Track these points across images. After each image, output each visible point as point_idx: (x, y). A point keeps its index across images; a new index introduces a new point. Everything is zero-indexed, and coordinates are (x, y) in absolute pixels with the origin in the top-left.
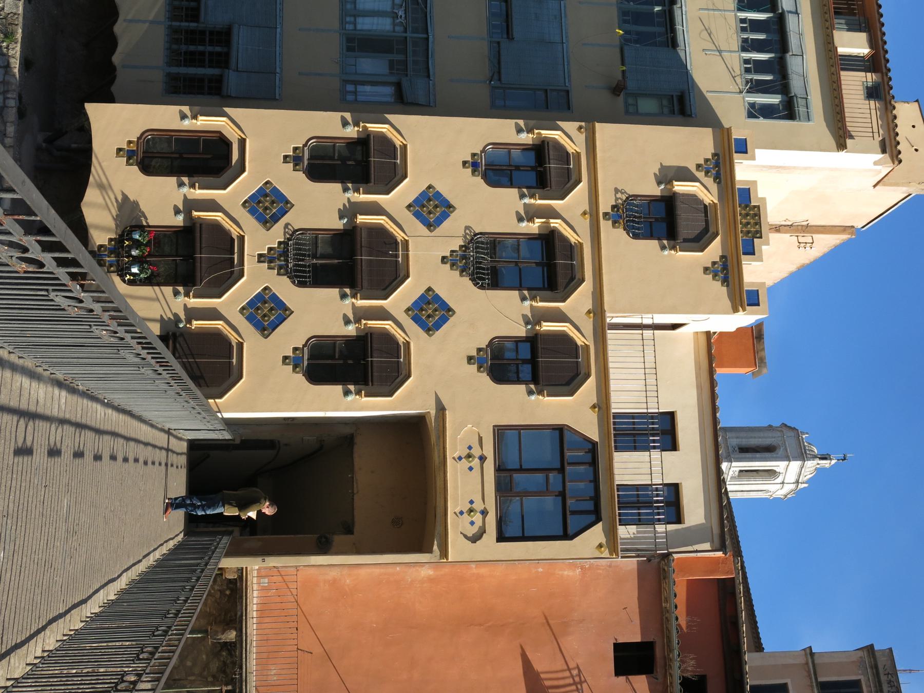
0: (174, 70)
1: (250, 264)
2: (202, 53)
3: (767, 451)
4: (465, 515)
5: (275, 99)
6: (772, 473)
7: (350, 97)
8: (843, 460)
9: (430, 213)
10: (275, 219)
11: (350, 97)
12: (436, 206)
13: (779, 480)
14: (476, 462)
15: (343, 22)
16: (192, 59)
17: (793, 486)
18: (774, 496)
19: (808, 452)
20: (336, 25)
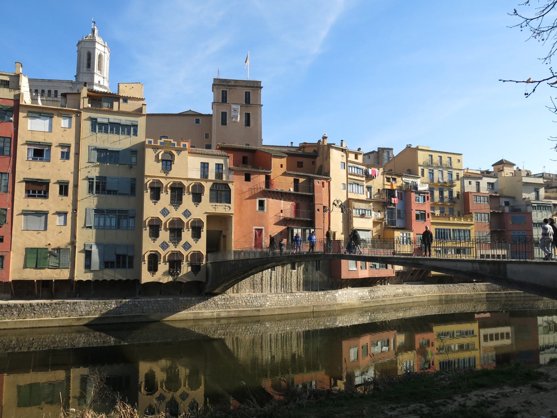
0: (127, 266)
1: (177, 249)
2: (123, 261)
3: (90, 57)
6: (100, 56)
8: (95, 23)
10: (167, 244)
11: (133, 228)
13: (103, 54)
14: (216, 207)
15: (113, 229)
16: (124, 263)
17: (106, 48)
18: (109, 57)
19: (91, 39)
20: (115, 231)
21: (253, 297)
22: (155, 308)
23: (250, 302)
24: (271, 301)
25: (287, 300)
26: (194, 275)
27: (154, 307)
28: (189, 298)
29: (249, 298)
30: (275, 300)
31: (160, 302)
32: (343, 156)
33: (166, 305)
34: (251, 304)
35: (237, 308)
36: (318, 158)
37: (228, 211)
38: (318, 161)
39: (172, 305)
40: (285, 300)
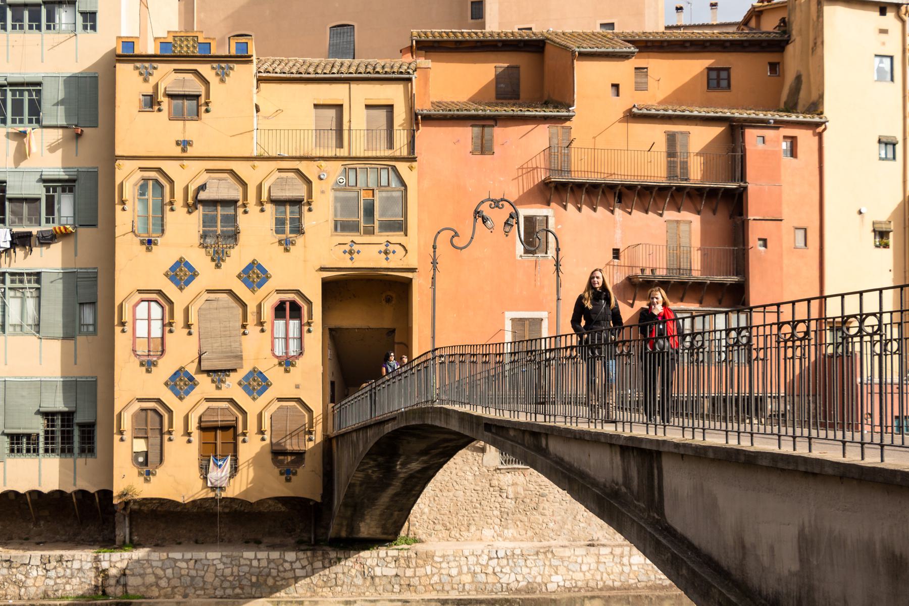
0: (76, 450)
1: (224, 393)
2: (63, 432)
4: (389, 256)
5: (96, 381)
9: (185, 275)
10: (191, 379)
11: (91, 329)
12: (181, 270)
14: (356, 248)
16: (67, 437)
21: (501, 554)
22: (163, 583)
23: (490, 570)
24: (568, 570)
25: (635, 568)
26: (284, 477)
27: (161, 578)
28: (275, 555)
29: (486, 558)
30: (585, 568)
31: (179, 564)
32: (884, 31)
33: (202, 573)
34: (491, 579)
35: (443, 590)
36: (790, 49)
37: (396, 261)
38: (792, 58)
39: (219, 573)
40: (627, 569)
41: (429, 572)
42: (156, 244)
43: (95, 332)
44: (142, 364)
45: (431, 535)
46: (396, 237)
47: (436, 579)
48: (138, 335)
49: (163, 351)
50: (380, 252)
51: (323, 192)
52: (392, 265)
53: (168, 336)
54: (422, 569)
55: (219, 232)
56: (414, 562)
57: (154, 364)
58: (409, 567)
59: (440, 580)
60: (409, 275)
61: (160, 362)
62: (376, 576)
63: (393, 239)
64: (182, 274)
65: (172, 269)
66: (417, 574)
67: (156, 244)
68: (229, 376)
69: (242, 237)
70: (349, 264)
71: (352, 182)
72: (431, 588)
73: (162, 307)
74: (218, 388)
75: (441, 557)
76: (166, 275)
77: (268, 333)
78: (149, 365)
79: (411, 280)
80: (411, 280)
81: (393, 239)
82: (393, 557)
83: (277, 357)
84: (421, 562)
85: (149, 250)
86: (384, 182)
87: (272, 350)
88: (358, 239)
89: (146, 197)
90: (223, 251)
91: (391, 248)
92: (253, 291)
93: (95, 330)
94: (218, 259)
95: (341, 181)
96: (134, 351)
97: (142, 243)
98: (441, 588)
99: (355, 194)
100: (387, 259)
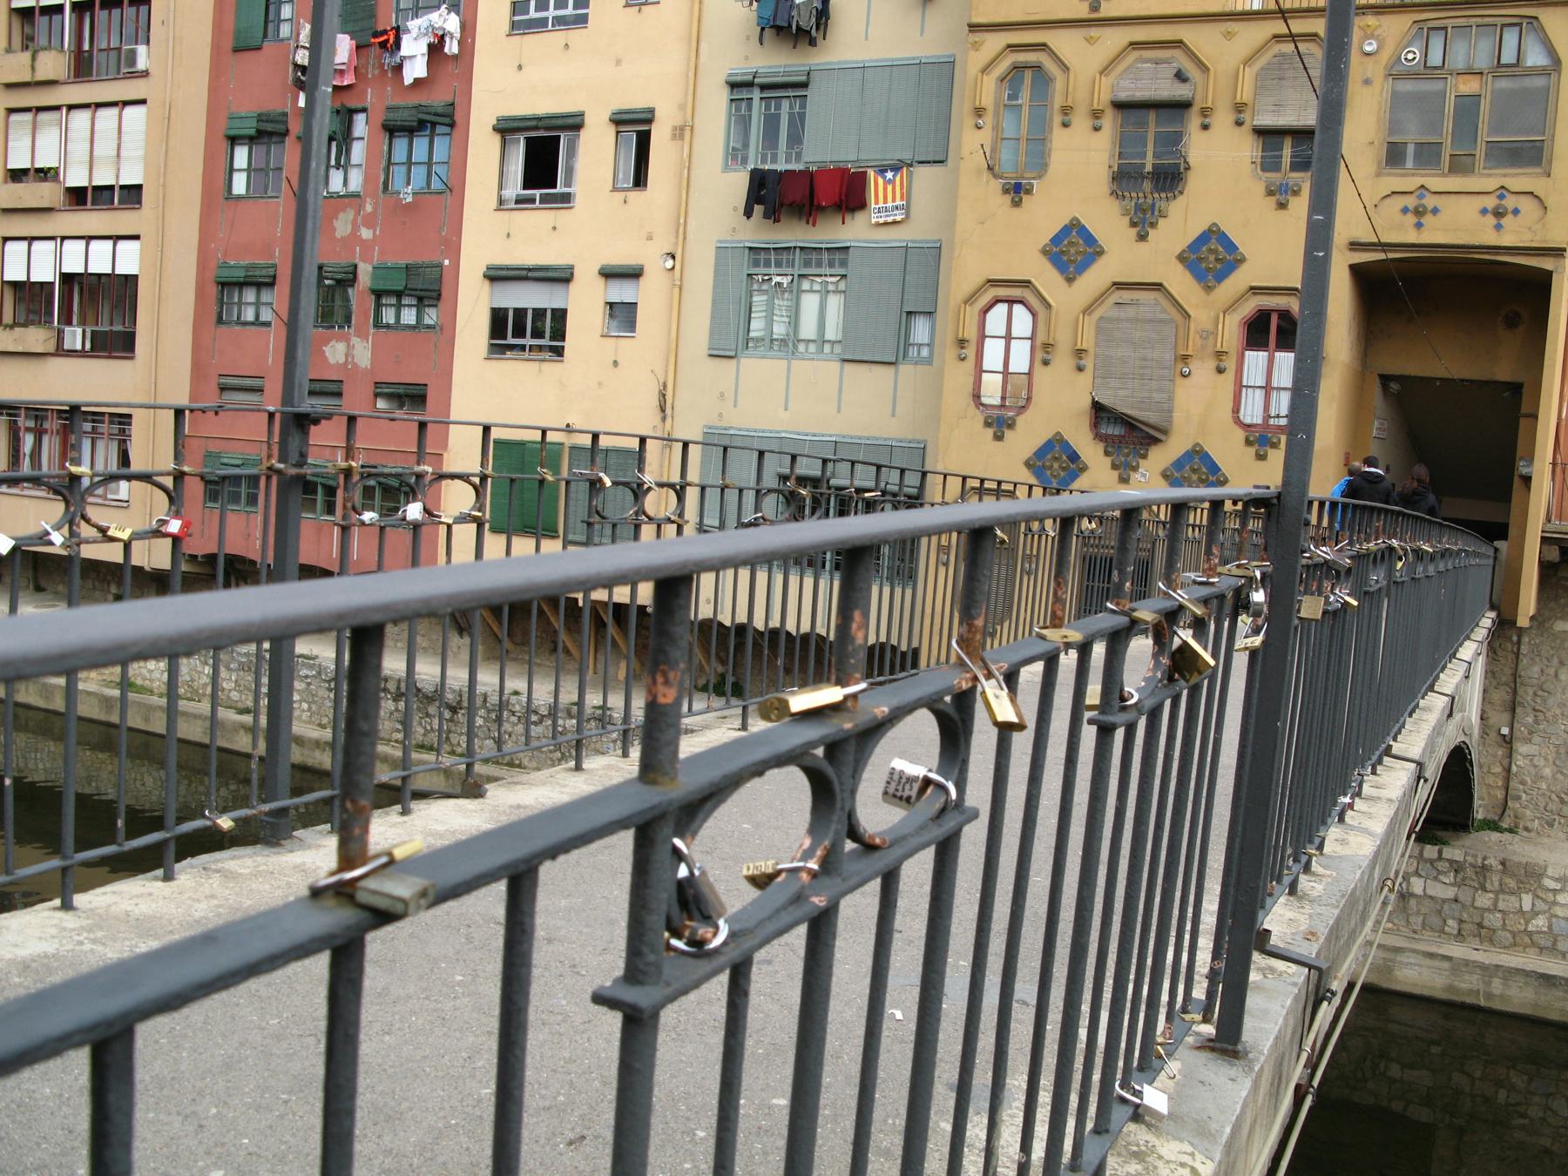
7: (925, 352)
11: (925, 352)
41: (1527, 906)
42: (1029, 192)
43: (929, 361)
44: (988, 424)
45: (1551, 825)
46: (1520, 180)
47: (1540, 923)
48: (1011, 370)
49: (1029, 399)
50: (1484, 211)
51: (1367, 82)
52: (1507, 240)
53: (1041, 373)
54: (1513, 898)
55: (1149, 168)
56: (1496, 879)
57: (1011, 425)
58: (1484, 889)
59: (1550, 927)
60: (1546, 264)
61: (1020, 421)
62: (1412, 895)
63: (1516, 184)
64: (1072, 251)
65: (1056, 240)
66: (1501, 905)
67: (1029, 192)
68: (1144, 457)
69: (1194, 182)
70: (1412, 237)
71: (1435, 58)
72: (1527, 940)
73: (1034, 314)
74: (1124, 480)
75: (1557, 880)
76: (1044, 252)
77: (1230, 376)
78: (999, 424)
79: (1549, 274)
80: (1549, 274)
81: (1516, 184)
82: (1451, 862)
83: (1247, 427)
84: (1512, 883)
85: (1017, 204)
86: (1508, 56)
87: (1236, 410)
88: (1435, 183)
89: (1020, 102)
90: (1153, 205)
91: (1510, 202)
92: (1208, 289)
93: (931, 352)
94: (1143, 222)
95: (1410, 56)
96: (977, 396)
97: (1006, 191)
98: (1549, 944)
99: (1438, 86)
100: (1498, 227)
